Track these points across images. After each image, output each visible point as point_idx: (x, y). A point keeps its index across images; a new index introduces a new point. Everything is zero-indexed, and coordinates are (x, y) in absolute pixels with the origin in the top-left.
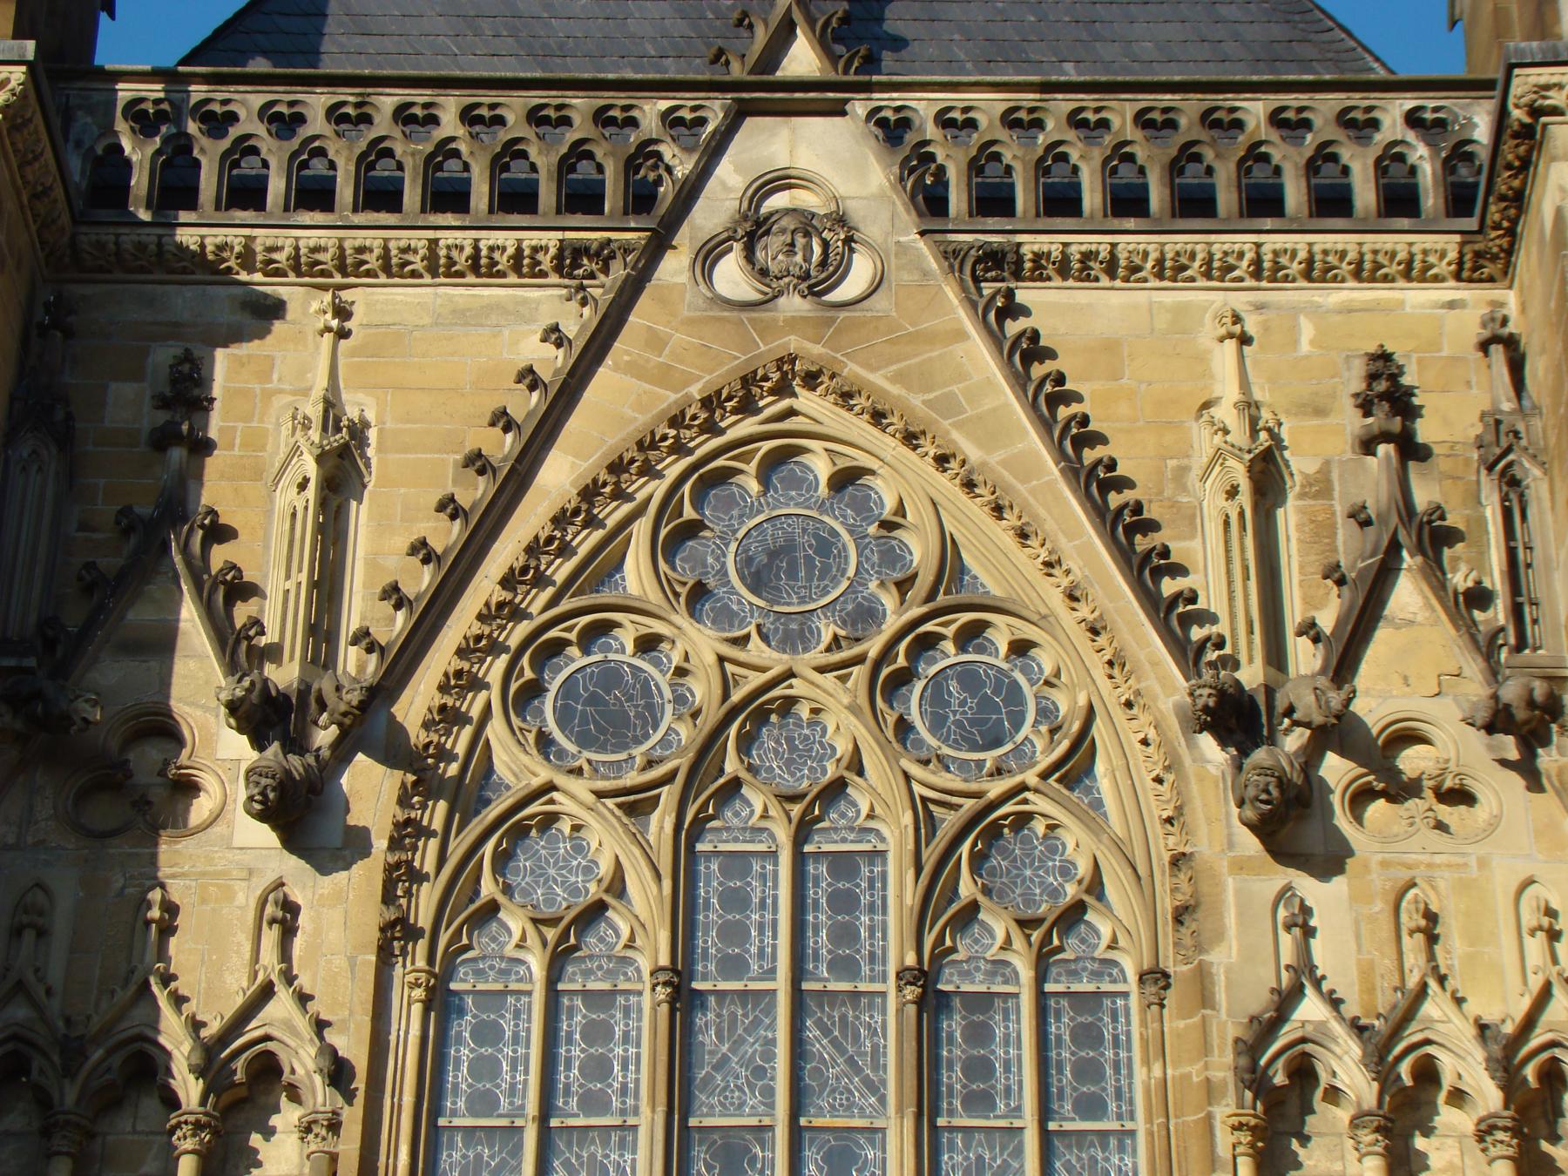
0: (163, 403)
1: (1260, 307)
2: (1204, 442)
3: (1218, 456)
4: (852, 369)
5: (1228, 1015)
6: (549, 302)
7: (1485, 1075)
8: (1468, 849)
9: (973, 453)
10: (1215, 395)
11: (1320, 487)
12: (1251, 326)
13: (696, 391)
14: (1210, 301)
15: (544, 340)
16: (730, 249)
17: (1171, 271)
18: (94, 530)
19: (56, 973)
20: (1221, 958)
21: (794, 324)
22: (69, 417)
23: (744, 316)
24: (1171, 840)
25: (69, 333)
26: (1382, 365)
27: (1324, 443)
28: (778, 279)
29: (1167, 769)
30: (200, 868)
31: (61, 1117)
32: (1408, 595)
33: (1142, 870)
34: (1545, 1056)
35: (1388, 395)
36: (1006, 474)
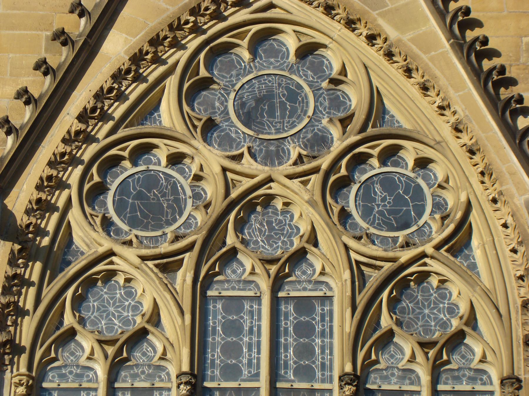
9: (392, 34)
24: (523, 291)
29: (520, 243)
33: (503, 310)
36: (414, 47)
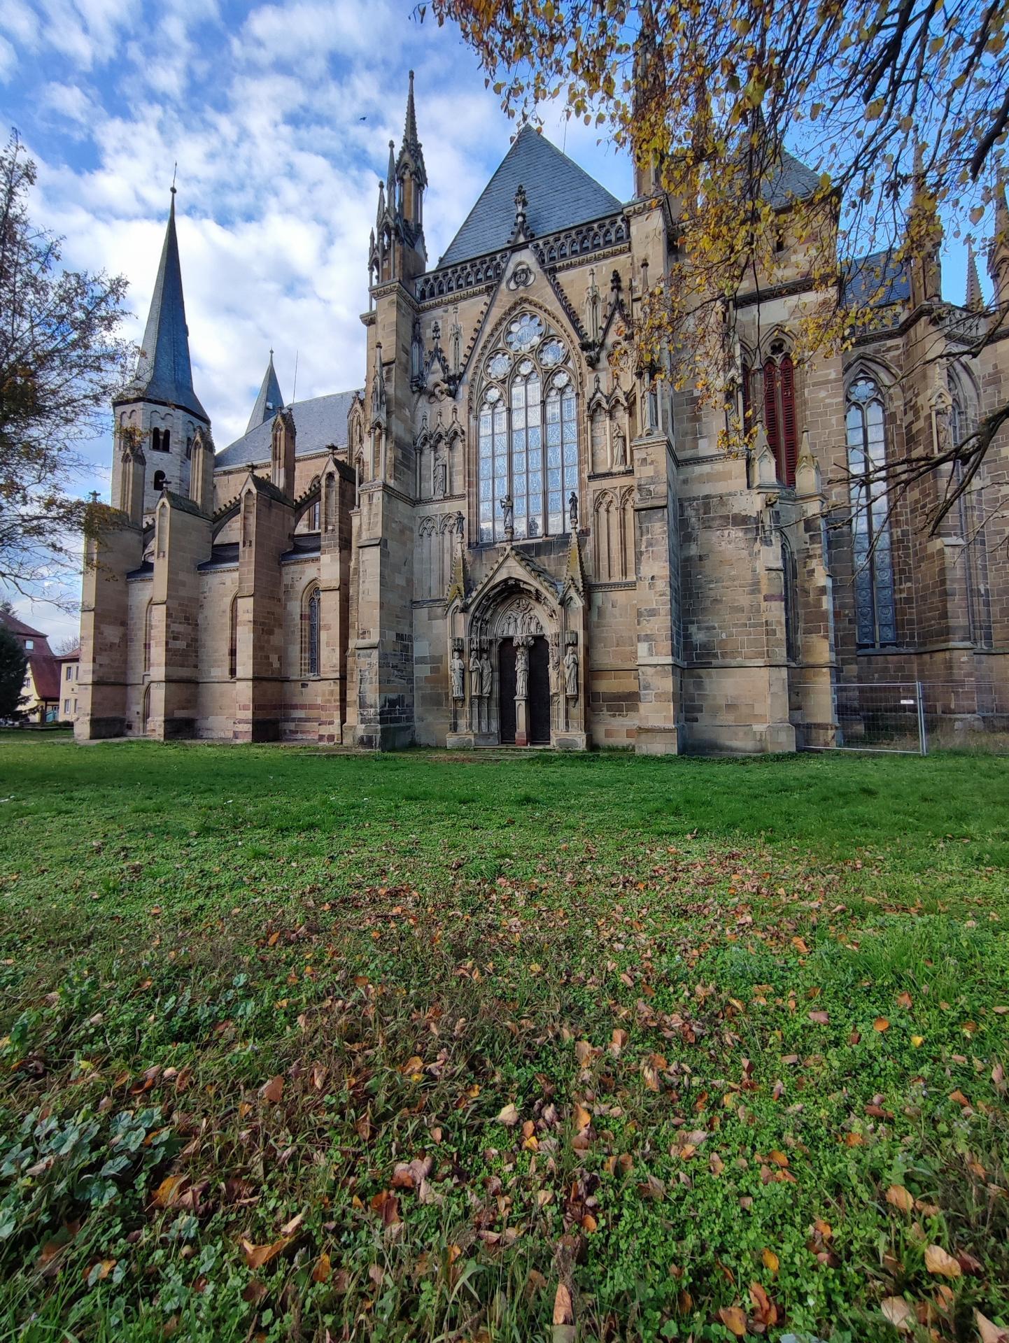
6: (486, 299)
14: (588, 268)
17: (581, 264)
27: (606, 292)
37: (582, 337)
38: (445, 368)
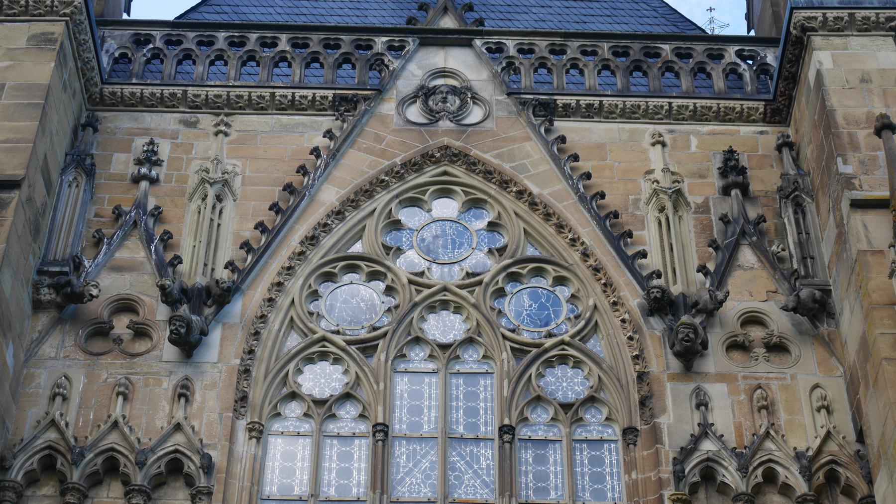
0: (139, 163)
1: (671, 132)
2: (646, 188)
3: (655, 192)
4: (475, 152)
5: (670, 447)
6: (327, 121)
7: (799, 477)
8: (786, 371)
9: (535, 190)
10: (652, 168)
11: (703, 208)
12: (667, 138)
13: (398, 160)
14: (647, 129)
15: (324, 137)
16: (415, 102)
17: (628, 115)
18: (102, 217)
19: (71, 417)
20: (665, 421)
21: (446, 132)
22: (93, 165)
23: (422, 129)
24: (637, 367)
25: (96, 130)
26: (730, 154)
27: (703, 189)
28: (438, 113)
29: (635, 332)
30: (145, 370)
31: (71, 485)
32: (747, 256)
33: (624, 382)
34: (827, 468)
35: (733, 172)
36: (551, 199)
37: (643, 281)
38: (167, 265)
